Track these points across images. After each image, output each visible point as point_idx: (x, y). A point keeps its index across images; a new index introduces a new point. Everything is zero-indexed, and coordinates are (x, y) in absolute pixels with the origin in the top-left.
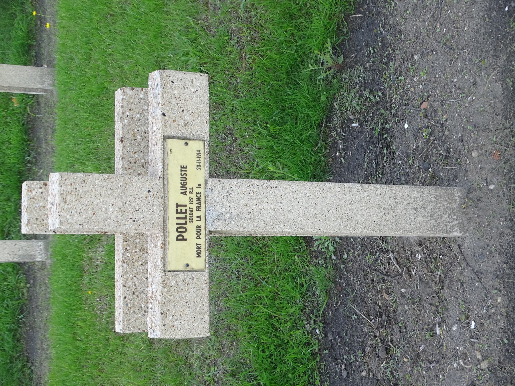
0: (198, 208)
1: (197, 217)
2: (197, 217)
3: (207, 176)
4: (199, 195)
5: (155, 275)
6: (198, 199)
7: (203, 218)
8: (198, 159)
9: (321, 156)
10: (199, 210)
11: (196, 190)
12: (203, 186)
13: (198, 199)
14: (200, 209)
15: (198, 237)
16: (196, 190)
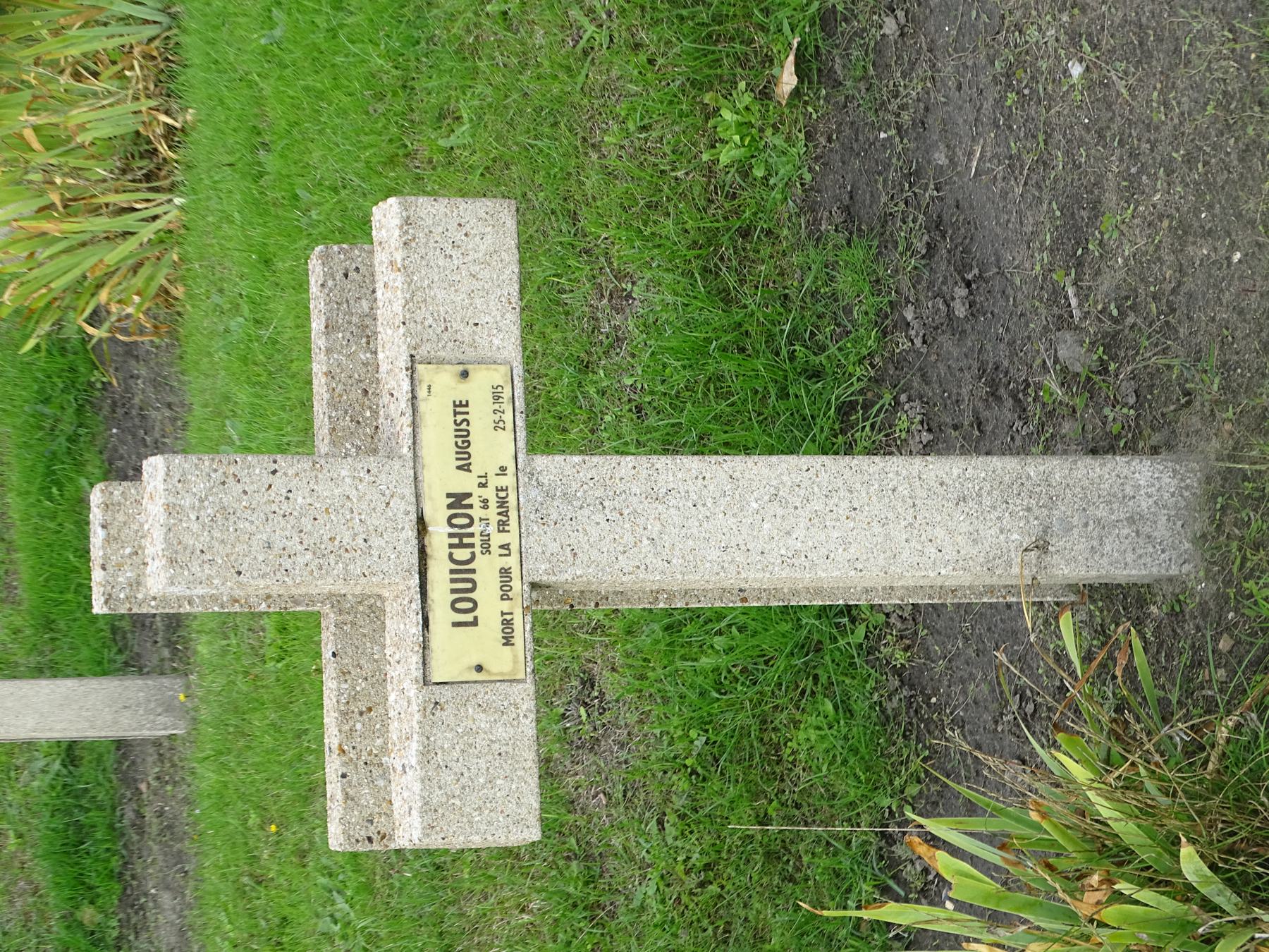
0: (502, 526)
1: (502, 547)
2: (502, 547)
3: (521, 444)
4: (502, 494)
5: (403, 696)
6: (502, 503)
7: (514, 547)
8: (497, 406)
9: (796, 387)
10: (504, 531)
11: (494, 482)
12: (511, 469)
13: (502, 503)
14: (507, 528)
15: (505, 597)
16: (494, 482)
